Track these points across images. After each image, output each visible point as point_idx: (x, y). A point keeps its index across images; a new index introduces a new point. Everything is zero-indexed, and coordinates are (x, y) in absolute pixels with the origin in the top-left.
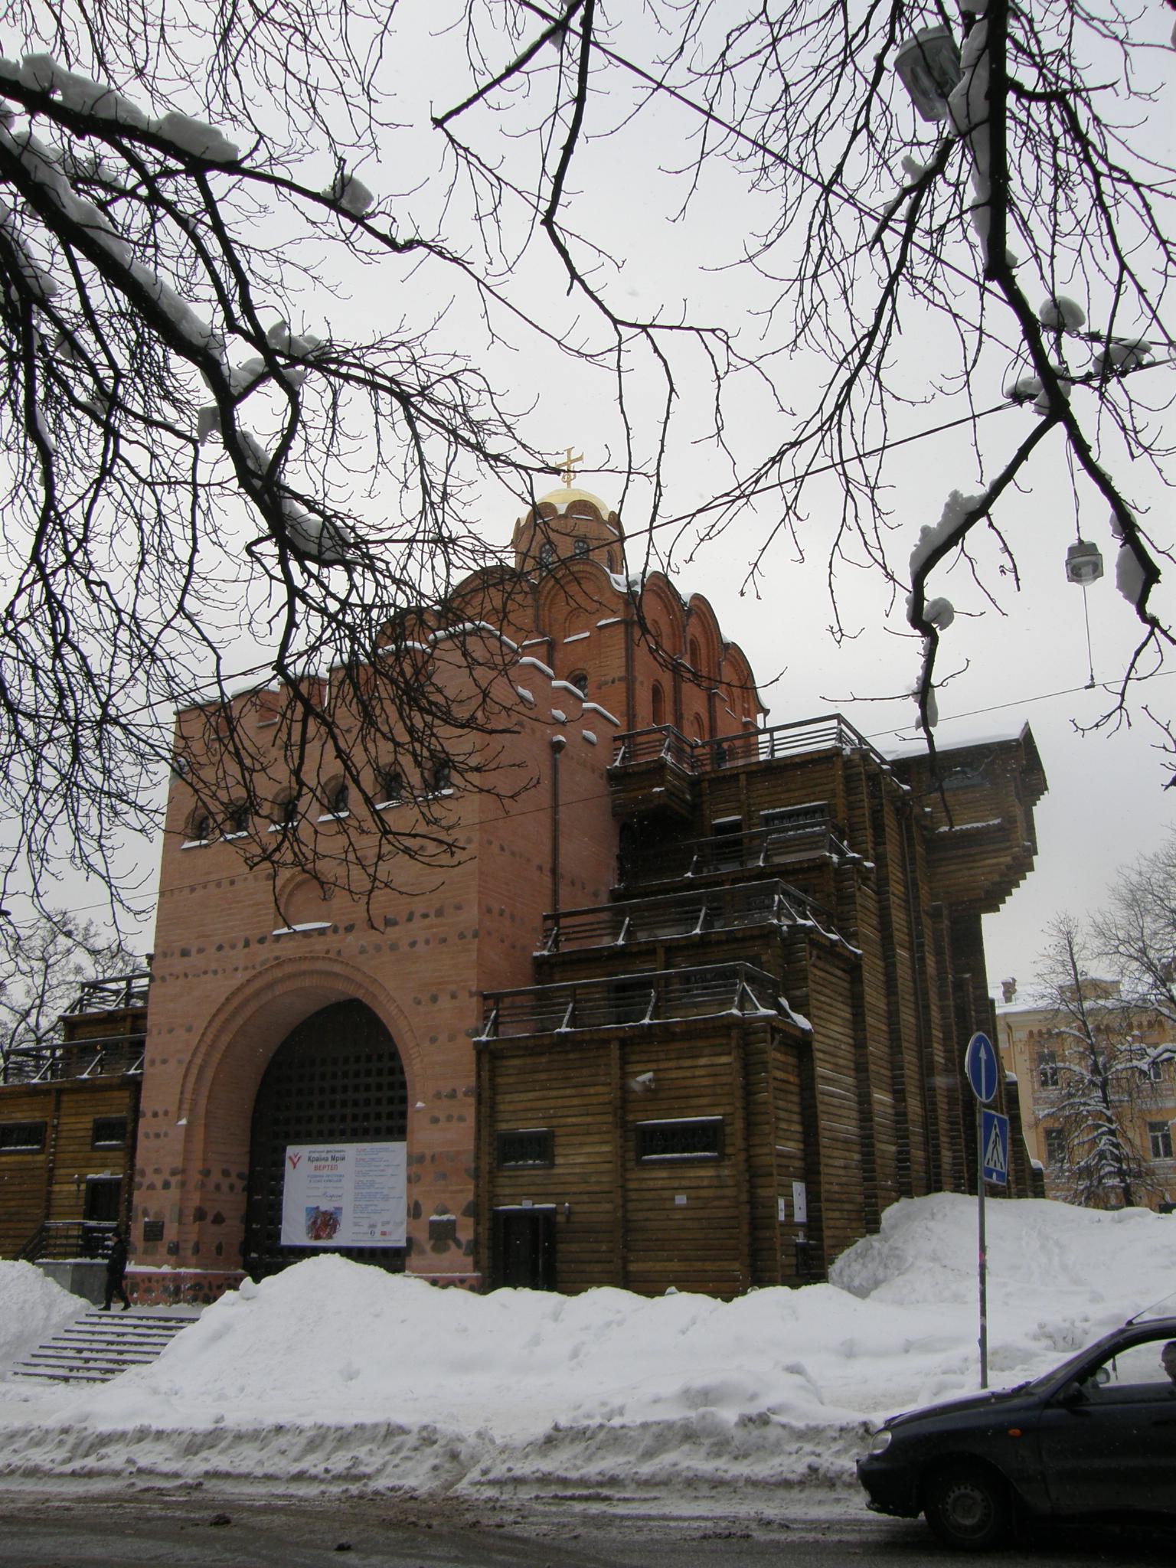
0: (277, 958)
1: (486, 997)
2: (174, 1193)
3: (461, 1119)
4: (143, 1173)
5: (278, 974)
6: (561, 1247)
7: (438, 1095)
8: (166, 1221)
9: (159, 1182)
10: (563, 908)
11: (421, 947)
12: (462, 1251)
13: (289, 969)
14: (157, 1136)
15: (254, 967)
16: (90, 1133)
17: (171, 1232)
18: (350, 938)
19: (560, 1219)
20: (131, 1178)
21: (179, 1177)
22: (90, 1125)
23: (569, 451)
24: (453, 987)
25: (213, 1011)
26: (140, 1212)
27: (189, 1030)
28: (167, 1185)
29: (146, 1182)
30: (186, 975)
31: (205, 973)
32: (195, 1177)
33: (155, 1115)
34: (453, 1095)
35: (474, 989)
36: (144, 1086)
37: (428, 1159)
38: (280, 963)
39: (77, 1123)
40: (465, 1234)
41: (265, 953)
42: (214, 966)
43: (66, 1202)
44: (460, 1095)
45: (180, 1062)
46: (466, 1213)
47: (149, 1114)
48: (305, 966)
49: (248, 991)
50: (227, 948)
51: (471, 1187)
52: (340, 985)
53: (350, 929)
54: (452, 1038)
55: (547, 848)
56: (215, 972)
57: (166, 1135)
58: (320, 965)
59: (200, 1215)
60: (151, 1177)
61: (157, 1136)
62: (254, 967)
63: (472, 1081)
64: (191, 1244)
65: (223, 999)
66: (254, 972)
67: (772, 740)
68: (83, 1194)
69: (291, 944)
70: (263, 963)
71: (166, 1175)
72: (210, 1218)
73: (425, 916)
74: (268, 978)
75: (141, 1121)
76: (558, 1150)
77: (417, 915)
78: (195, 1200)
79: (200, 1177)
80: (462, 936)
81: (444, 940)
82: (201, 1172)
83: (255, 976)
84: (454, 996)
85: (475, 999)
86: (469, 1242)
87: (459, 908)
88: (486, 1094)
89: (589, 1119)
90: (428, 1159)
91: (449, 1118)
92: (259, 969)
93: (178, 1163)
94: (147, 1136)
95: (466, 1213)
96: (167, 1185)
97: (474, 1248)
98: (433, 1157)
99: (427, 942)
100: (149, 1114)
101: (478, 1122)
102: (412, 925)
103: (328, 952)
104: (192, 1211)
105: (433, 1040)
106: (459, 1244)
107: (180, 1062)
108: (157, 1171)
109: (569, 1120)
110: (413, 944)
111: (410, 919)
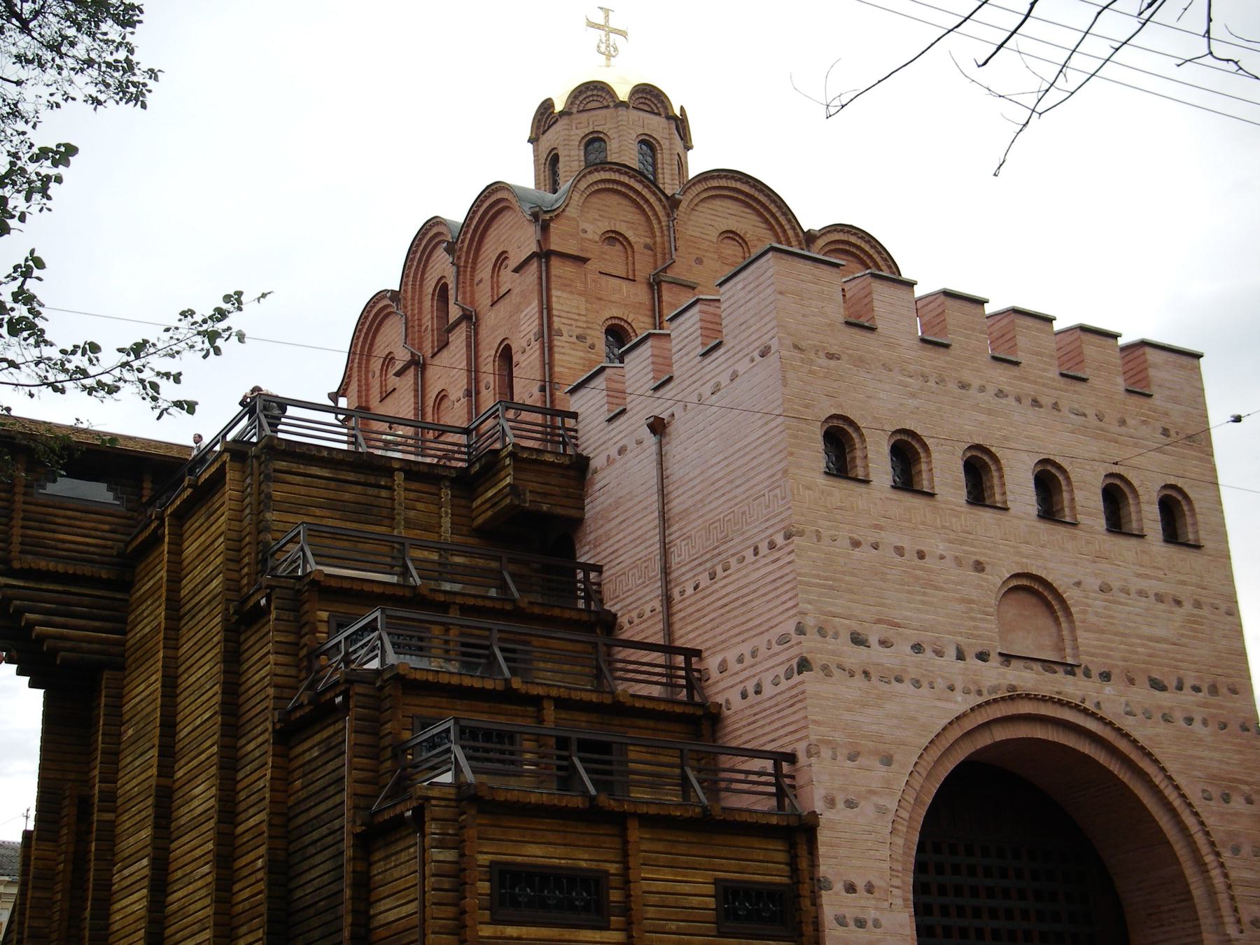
11: (1197, 725)
13: (1026, 708)
14: (861, 923)
15: (979, 693)
18: (1108, 689)
25: (925, 742)
27: (888, 761)
30: (866, 674)
31: (899, 680)
33: (851, 888)
38: (1014, 696)
41: (995, 676)
42: (913, 673)
45: (882, 811)
47: (839, 887)
49: (968, 725)
50: (929, 654)
53: (1106, 676)
56: (917, 684)
57: (877, 924)
61: (861, 923)
62: (979, 693)
65: (938, 729)
66: (980, 700)
69: (1027, 674)
70: (994, 689)
73: (1197, 689)
75: (826, 897)
83: (979, 706)
94: (841, 921)
99: (1205, 723)
100: (839, 887)
105: (1236, 850)
107: (882, 811)
110: (1189, 721)
111: (1180, 687)
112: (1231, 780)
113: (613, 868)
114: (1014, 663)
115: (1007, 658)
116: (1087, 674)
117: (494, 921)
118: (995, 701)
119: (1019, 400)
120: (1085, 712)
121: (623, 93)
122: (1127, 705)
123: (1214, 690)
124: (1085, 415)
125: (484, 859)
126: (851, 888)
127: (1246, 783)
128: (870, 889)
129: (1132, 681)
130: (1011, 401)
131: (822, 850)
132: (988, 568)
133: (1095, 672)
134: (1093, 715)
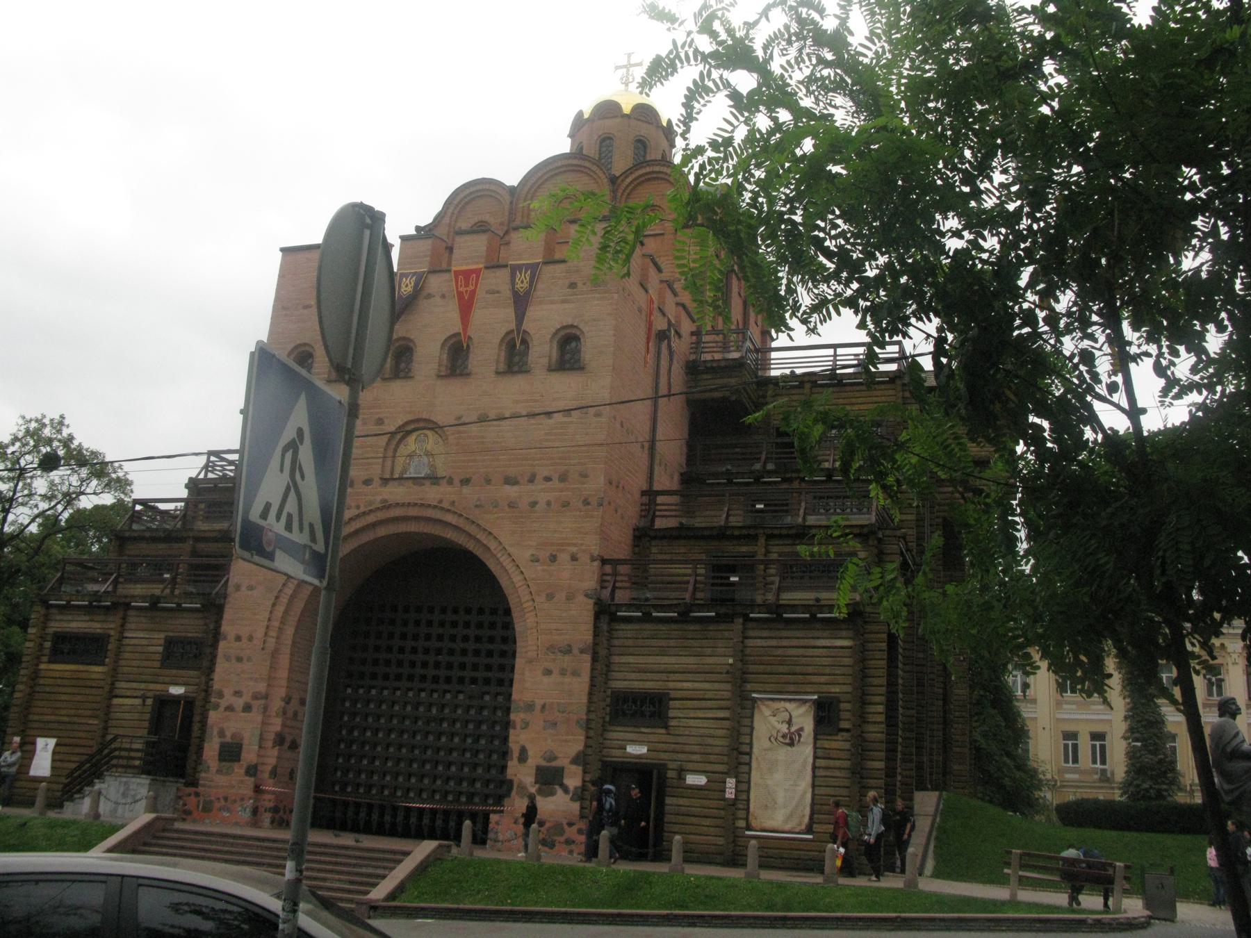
0: (385, 501)
1: (604, 562)
2: (256, 716)
3: (575, 673)
4: (220, 695)
5: (381, 515)
6: (668, 800)
7: (551, 648)
8: (245, 742)
9: (239, 703)
10: (657, 487)
11: (541, 506)
12: (568, 797)
14: (239, 659)
15: (358, 507)
16: (160, 649)
17: (250, 755)
18: (466, 490)
19: (671, 774)
20: (206, 700)
21: (263, 702)
22: (162, 642)
23: (629, 55)
24: (574, 549)
26: (215, 733)
28: (247, 708)
29: (223, 703)
32: (277, 704)
33: (238, 638)
34: (568, 650)
35: (596, 554)
36: (226, 610)
37: (538, 707)
38: (386, 506)
39: (144, 639)
40: (573, 780)
43: (127, 716)
44: (576, 651)
46: (575, 761)
47: (231, 636)
48: (413, 512)
51: (582, 738)
52: (450, 535)
53: (466, 482)
54: (570, 597)
55: (647, 427)
58: (429, 513)
59: (280, 740)
60: (229, 699)
62: (358, 507)
63: (589, 638)
64: (269, 768)
66: (357, 512)
67: (835, 355)
68: (149, 709)
71: (246, 698)
72: (287, 744)
73: (548, 479)
74: (371, 519)
76: (671, 713)
77: (539, 478)
78: (276, 725)
79: (283, 704)
80: (586, 502)
81: (566, 504)
82: (283, 700)
83: (358, 516)
84: (574, 558)
85: (596, 563)
86: (576, 788)
87: (584, 475)
88: (602, 652)
89: (707, 686)
90: (538, 707)
91: (563, 672)
92: (362, 509)
93: (261, 687)
95: (575, 761)
96: (247, 708)
97: (579, 795)
98: (544, 707)
99: (549, 504)
101: (592, 678)
102: (531, 487)
103: (441, 501)
104: (272, 736)
105: (550, 597)
106: (566, 790)
108: (238, 693)
109: (686, 685)
111: (532, 480)
112: (562, 545)
113: (112, 633)
114: (391, 483)
115: (385, 481)
116: (450, 482)
117: (50, 662)
118: (371, 511)
119: (443, 296)
120: (442, 509)
121: (627, 109)
122: (479, 499)
123: (563, 478)
124: (498, 292)
125: (51, 631)
126: (238, 638)
127: (575, 545)
128: (250, 638)
129: (488, 481)
130: (438, 299)
131: (226, 616)
132: (386, 421)
133: (457, 482)
134: (449, 511)
